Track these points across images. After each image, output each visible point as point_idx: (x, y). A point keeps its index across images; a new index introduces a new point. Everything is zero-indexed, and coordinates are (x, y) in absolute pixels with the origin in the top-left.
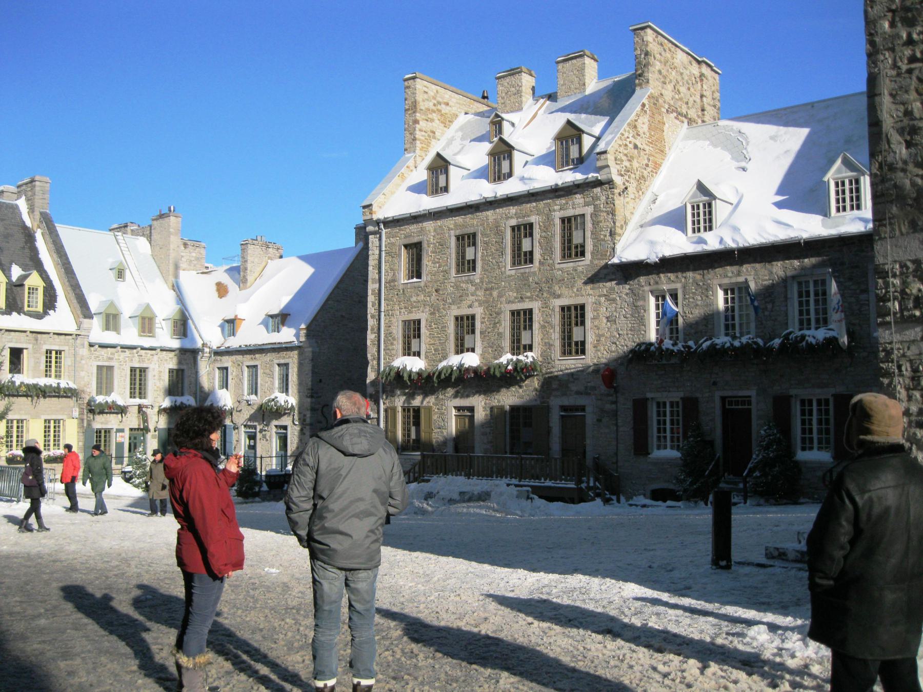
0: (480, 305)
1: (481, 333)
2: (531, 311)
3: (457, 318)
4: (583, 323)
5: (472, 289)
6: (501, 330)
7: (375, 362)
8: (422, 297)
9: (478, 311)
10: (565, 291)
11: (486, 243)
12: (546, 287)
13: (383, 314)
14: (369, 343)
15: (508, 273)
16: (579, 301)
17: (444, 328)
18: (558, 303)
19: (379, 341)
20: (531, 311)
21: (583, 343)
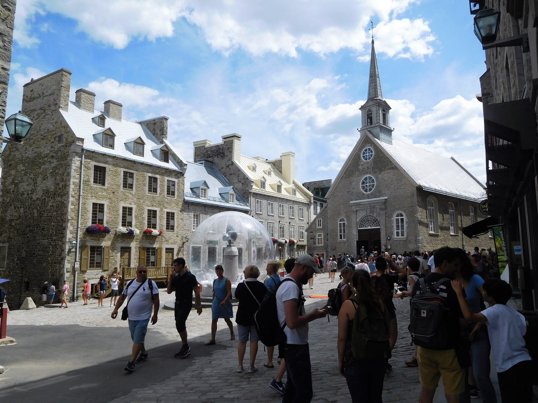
0: (135, 204)
1: (135, 216)
2: (155, 211)
3: (124, 208)
4: (173, 219)
5: (130, 196)
6: (144, 216)
7: (75, 222)
8: (104, 194)
9: (134, 207)
10: (167, 206)
11: (137, 179)
12: (161, 204)
13: (81, 197)
14: (69, 210)
15: (147, 194)
16: (173, 211)
17: (117, 211)
18: (166, 210)
19: (79, 210)
20: (155, 211)
21: (173, 226)
